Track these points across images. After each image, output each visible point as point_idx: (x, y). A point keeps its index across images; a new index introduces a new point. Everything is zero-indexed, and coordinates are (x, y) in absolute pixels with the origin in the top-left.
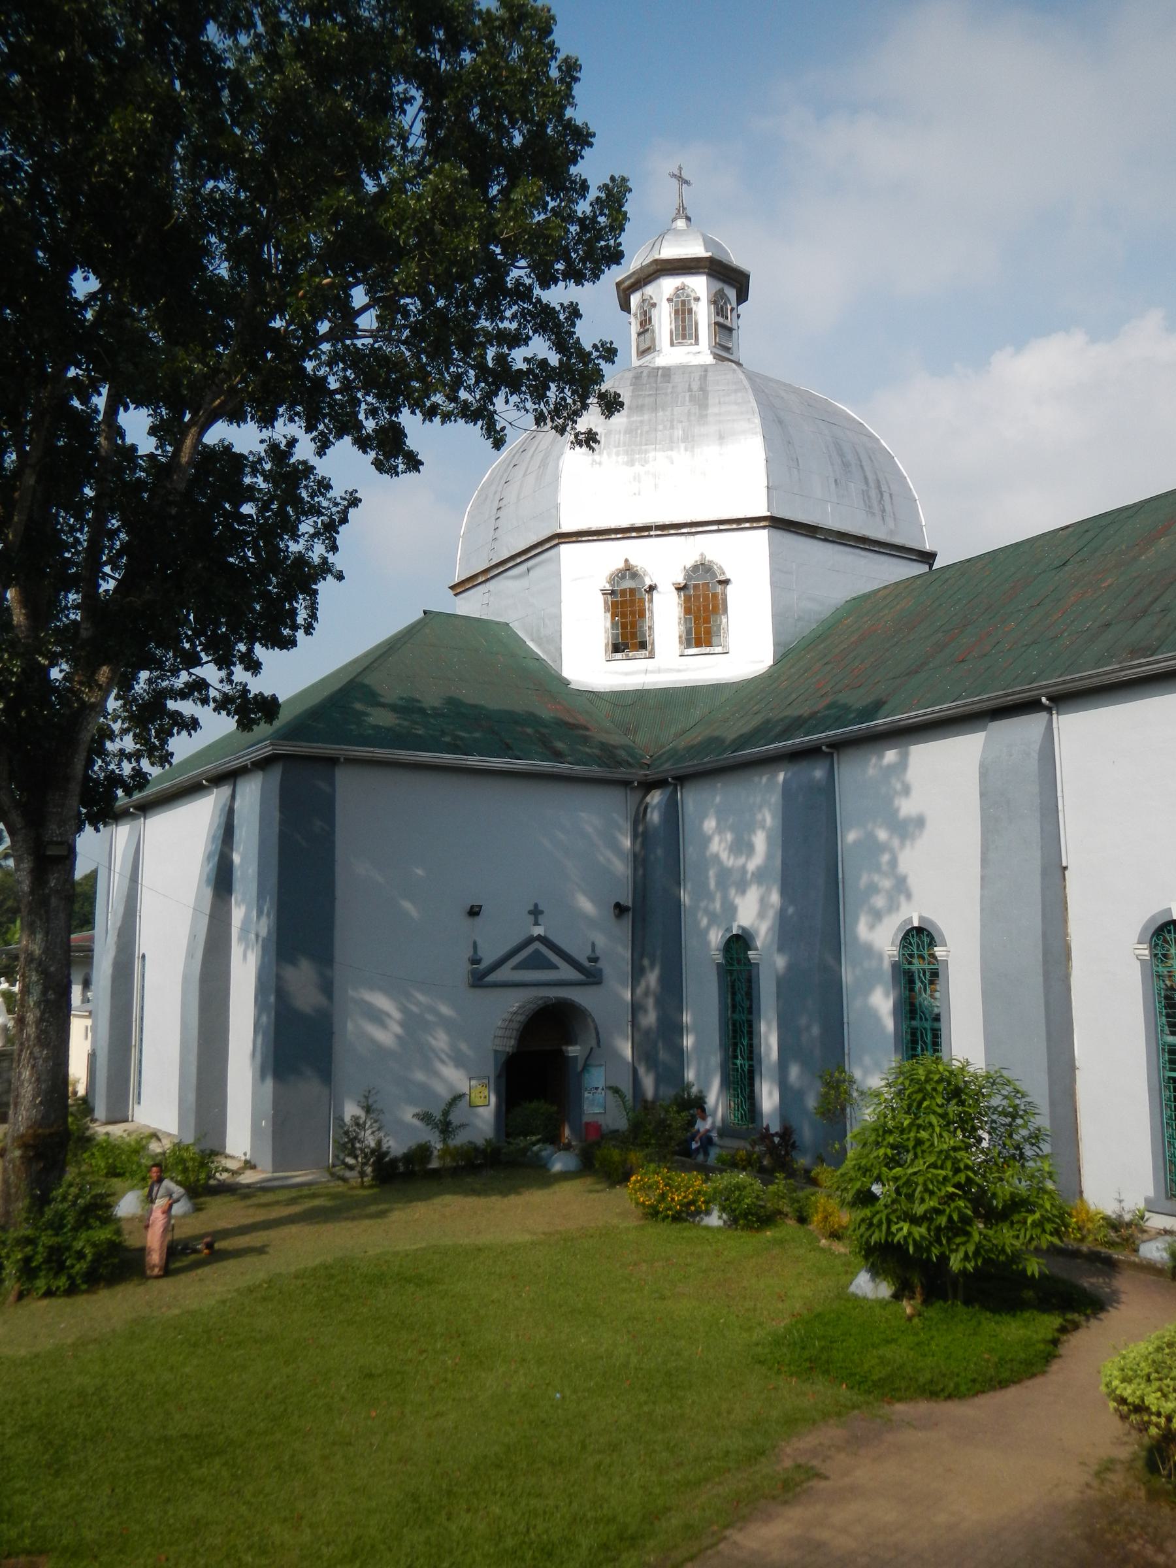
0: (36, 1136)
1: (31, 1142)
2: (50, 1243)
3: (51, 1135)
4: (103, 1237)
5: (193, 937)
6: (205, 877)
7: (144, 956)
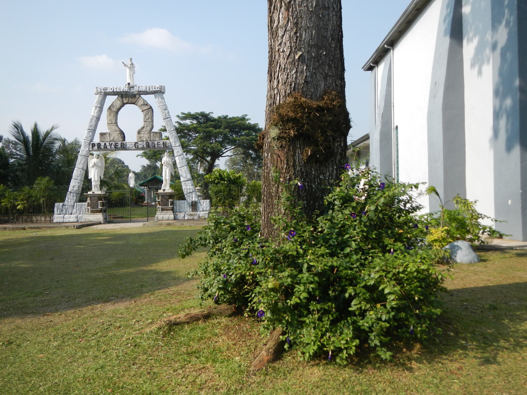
0: (298, 106)
1: (291, 114)
2: (319, 268)
3: (320, 109)
4: (412, 267)
5: (434, 84)
6: (443, 27)
7: (397, 127)
